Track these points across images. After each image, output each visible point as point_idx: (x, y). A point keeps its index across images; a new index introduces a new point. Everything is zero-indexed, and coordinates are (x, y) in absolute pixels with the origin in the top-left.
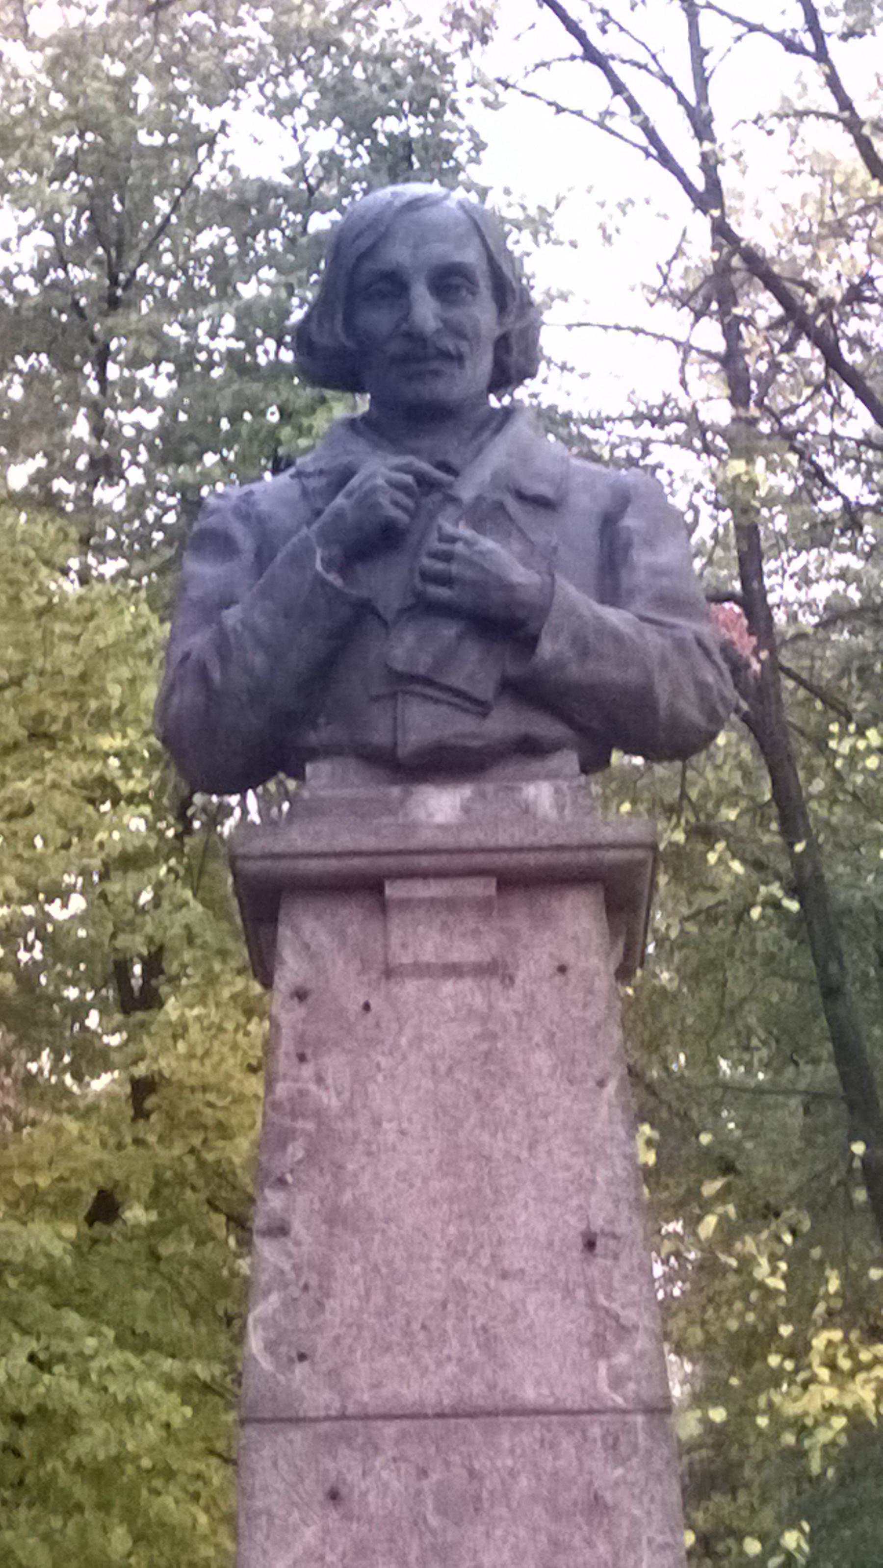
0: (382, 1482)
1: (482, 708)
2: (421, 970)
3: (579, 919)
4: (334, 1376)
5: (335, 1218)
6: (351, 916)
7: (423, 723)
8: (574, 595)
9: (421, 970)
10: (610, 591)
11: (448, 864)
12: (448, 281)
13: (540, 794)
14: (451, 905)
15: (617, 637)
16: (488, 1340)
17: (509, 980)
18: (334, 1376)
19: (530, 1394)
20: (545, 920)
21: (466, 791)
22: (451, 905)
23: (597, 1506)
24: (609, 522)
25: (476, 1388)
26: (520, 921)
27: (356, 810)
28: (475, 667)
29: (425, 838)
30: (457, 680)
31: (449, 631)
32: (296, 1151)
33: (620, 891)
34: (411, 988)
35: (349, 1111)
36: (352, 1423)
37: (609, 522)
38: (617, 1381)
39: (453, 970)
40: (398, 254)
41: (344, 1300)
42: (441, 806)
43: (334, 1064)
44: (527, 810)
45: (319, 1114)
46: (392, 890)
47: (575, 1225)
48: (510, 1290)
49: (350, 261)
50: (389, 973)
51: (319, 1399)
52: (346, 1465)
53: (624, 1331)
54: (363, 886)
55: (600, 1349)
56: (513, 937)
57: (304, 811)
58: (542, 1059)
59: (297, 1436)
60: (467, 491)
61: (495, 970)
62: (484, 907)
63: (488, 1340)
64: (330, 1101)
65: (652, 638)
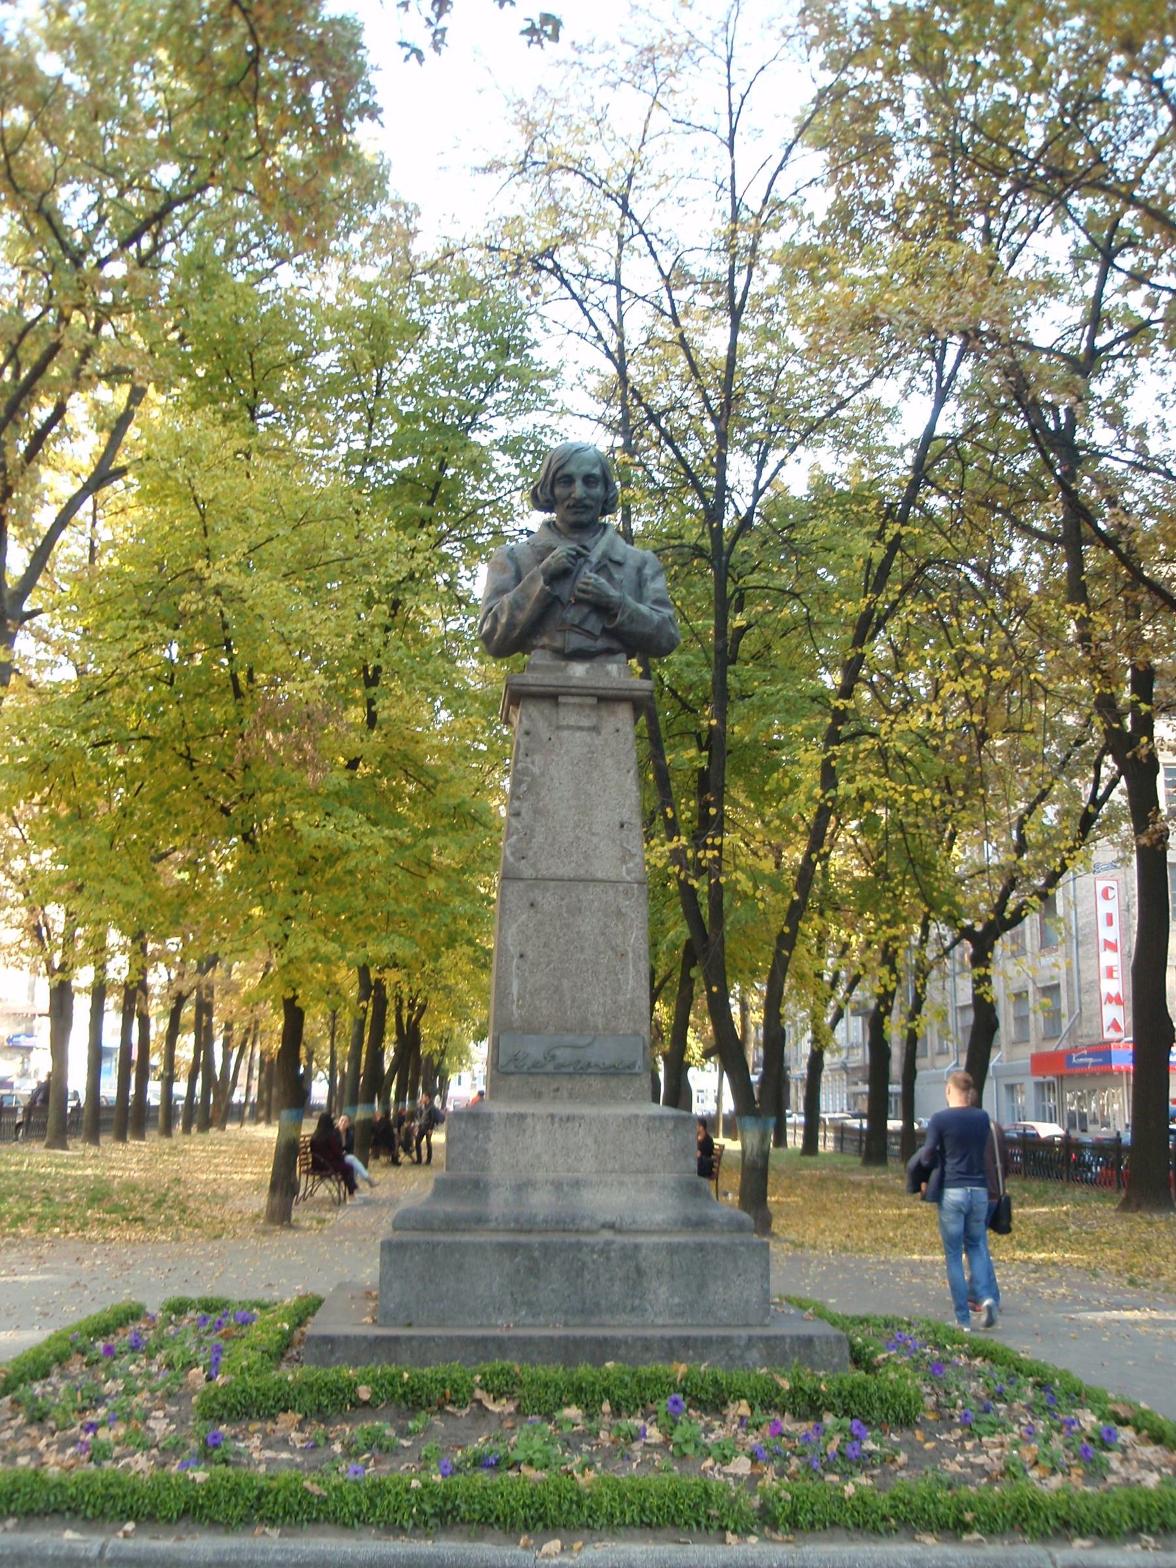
0: (548, 901)
1: (595, 638)
2: (569, 727)
3: (624, 714)
4: (534, 865)
5: (537, 812)
6: (546, 707)
7: (576, 641)
8: (630, 600)
9: (569, 727)
10: (640, 599)
11: (581, 692)
12: (588, 480)
13: (613, 668)
14: (581, 706)
15: (643, 616)
16: (587, 857)
17: (599, 733)
18: (534, 865)
19: (600, 875)
20: (613, 713)
21: (587, 665)
22: (581, 706)
23: (619, 914)
24: (639, 570)
25: (582, 871)
26: (604, 713)
27: (548, 668)
28: (594, 624)
29: (574, 682)
30: (588, 627)
31: (586, 610)
32: (524, 787)
33: (640, 705)
34: (565, 733)
35: (542, 774)
36: (540, 881)
37: (639, 570)
38: (629, 872)
39: (581, 728)
40: (571, 469)
41: (538, 840)
42: (578, 670)
43: (537, 758)
44: (608, 674)
45: (533, 775)
46: (561, 699)
47: (617, 819)
48: (595, 840)
49: (553, 468)
50: (559, 728)
51: (528, 872)
52: (537, 895)
53: (633, 856)
54: (551, 697)
55: (624, 861)
56: (600, 718)
57: (527, 667)
58: (609, 762)
59: (521, 884)
60: (595, 556)
61: (595, 729)
62: (592, 707)
63: (587, 857)
64: (536, 770)
65: (656, 617)
